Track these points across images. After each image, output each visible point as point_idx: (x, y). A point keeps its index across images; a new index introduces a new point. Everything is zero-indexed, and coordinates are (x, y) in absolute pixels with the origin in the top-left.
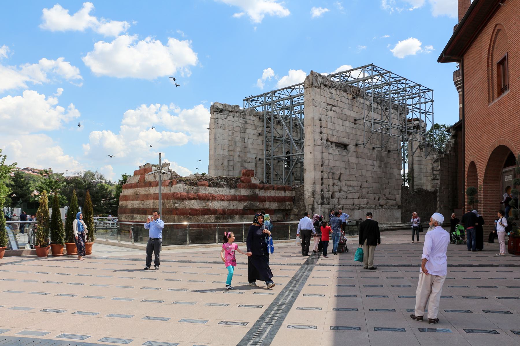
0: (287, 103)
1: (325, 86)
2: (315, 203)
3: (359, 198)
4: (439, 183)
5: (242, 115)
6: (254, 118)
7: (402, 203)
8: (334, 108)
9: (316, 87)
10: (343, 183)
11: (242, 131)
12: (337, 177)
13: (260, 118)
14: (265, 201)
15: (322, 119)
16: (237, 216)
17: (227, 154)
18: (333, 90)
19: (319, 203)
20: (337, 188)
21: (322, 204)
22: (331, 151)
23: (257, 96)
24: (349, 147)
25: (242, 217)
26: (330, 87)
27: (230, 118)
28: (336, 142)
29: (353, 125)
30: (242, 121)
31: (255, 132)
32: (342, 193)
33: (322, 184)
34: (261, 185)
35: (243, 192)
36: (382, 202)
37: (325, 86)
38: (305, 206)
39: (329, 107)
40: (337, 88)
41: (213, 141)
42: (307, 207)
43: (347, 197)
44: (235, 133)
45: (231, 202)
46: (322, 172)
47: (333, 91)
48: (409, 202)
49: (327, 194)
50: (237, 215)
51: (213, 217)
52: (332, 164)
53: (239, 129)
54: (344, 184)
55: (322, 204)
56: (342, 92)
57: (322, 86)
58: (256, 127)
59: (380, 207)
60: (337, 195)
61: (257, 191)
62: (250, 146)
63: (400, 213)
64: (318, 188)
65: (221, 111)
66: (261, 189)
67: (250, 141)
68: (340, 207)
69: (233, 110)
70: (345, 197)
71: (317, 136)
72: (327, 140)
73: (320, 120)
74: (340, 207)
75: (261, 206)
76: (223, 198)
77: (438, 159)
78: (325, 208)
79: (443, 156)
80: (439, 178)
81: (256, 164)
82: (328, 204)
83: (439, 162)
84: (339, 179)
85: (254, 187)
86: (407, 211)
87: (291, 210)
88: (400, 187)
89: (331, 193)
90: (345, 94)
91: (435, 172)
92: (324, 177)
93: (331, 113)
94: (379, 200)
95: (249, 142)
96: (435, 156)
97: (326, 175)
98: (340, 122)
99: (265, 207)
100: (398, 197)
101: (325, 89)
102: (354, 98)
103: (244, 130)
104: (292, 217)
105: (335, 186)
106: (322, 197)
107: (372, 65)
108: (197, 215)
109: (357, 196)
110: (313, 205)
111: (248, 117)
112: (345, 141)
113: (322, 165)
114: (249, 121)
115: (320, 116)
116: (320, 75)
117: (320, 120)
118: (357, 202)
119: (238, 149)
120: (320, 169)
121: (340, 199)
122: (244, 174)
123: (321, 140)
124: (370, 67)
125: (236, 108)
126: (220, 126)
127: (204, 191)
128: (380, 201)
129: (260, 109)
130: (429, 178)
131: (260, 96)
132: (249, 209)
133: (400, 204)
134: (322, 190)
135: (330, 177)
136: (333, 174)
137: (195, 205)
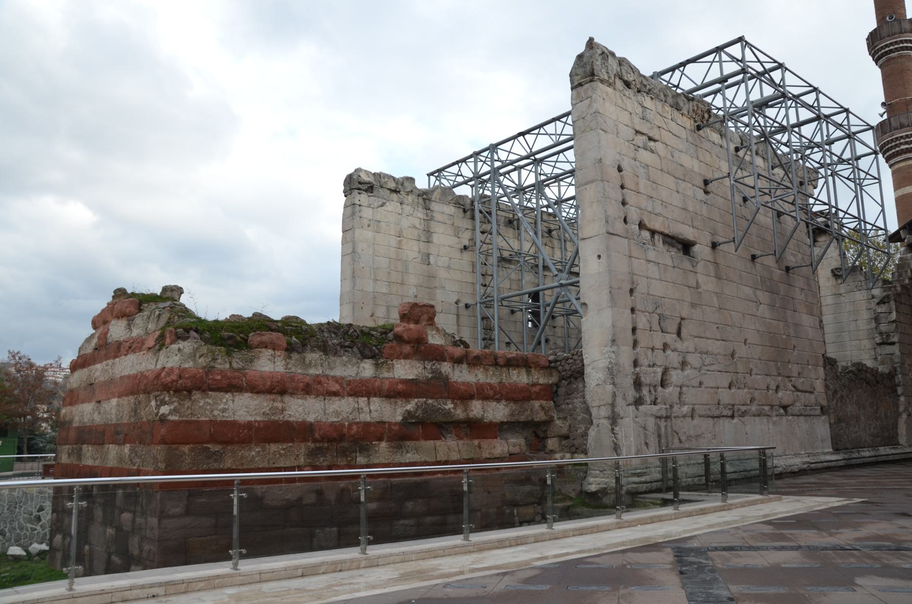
0: (528, 178)
1: (627, 84)
2: (619, 400)
3: (730, 388)
4: (898, 353)
5: (421, 200)
6: (451, 209)
7: (828, 401)
8: (652, 144)
9: (602, 81)
10: (688, 344)
11: (423, 238)
12: (674, 328)
13: (465, 211)
14: (471, 397)
15: (625, 165)
16: (383, 444)
17: (384, 290)
18: (648, 99)
19: (631, 399)
20: (674, 358)
21: (638, 402)
22: (652, 255)
23: (457, 163)
24: (696, 249)
25: (400, 447)
26: (639, 91)
27: (393, 206)
28: (662, 233)
29: (700, 194)
30: (420, 213)
31: (452, 241)
32: (688, 372)
33: (635, 344)
34: (459, 351)
35: (405, 370)
36: (785, 396)
37: (627, 84)
38: (588, 411)
39: (640, 140)
40: (657, 97)
41: (348, 258)
42: (594, 412)
43: (701, 383)
44: (405, 241)
45: (363, 401)
46: (633, 310)
47: (648, 102)
48: (842, 396)
49: (651, 376)
50: (380, 439)
51: (301, 450)
52: (658, 289)
53: (416, 232)
54: (691, 349)
55: (638, 402)
56: (668, 108)
57: (619, 84)
58: (457, 233)
59: (782, 411)
60: (675, 376)
61: (446, 368)
62: (442, 274)
63: (827, 426)
64: (626, 356)
65: (370, 188)
66: (458, 361)
67: (443, 261)
68: (685, 409)
69: (401, 187)
70: (695, 383)
71: (615, 210)
72: (642, 226)
73: (620, 169)
74: (685, 409)
75: (460, 414)
76: (335, 387)
77: (888, 296)
78: (646, 415)
79: (899, 289)
81: (458, 315)
82: (655, 403)
83: (892, 303)
84: (679, 334)
85: (437, 355)
86: (839, 420)
87: (549, 422)
88: (821, 363)
89: (659, 371)
90: (677, 114)
91: (883, 327)
92: (640, 326)
93: (644, 155)
94: (777, 391)
95: (440, 264)
96: (877, 292)
97: (644, 320)
98: (670, 181)
99: (471, 415)
100: (819, 385)
101: (627, 93)
102: (699, 128)
103: (427, 236)
104: (552, 443)
105: (669, 352)
106: (638, 384)
107: (741, 39)
108: (245, 442)
109: (725, 380)
110: (613, 405)
111: (434, 206)
112: (688, 233)
113: (632, 291)
114: (438, 216)
115: (618, 157)
116: (613, 54)
117: (620, 169)
118: (726, 396)
119: (412, 280)
120: (628, 301)
121: (684, 389)
122: (404, 317)
123: (625, 221)
124: (735, 51)
125: (406, 184)
126: (366, 222)
127: (269, 364)
128: (780, 394)
129: (465, 191)
130: (867, 344)
131: (464, 160)
132: (421, 423)
133: (824, 403)
134: (636, 364)
135: (656, 326)
136: (661, 317)
137: (243, 408)
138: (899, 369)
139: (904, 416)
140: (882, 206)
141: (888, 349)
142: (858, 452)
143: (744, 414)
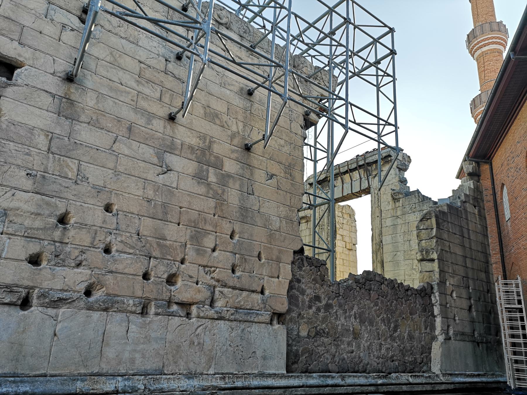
4: (437, 270)
48: (328, 307)
80: (435, 256)
133: (282, 307)
138: (436, 287)
139: (441, 338)
140: (395, 103)
141: (428, 266)
142: (343, 378)
143: (57, 303)
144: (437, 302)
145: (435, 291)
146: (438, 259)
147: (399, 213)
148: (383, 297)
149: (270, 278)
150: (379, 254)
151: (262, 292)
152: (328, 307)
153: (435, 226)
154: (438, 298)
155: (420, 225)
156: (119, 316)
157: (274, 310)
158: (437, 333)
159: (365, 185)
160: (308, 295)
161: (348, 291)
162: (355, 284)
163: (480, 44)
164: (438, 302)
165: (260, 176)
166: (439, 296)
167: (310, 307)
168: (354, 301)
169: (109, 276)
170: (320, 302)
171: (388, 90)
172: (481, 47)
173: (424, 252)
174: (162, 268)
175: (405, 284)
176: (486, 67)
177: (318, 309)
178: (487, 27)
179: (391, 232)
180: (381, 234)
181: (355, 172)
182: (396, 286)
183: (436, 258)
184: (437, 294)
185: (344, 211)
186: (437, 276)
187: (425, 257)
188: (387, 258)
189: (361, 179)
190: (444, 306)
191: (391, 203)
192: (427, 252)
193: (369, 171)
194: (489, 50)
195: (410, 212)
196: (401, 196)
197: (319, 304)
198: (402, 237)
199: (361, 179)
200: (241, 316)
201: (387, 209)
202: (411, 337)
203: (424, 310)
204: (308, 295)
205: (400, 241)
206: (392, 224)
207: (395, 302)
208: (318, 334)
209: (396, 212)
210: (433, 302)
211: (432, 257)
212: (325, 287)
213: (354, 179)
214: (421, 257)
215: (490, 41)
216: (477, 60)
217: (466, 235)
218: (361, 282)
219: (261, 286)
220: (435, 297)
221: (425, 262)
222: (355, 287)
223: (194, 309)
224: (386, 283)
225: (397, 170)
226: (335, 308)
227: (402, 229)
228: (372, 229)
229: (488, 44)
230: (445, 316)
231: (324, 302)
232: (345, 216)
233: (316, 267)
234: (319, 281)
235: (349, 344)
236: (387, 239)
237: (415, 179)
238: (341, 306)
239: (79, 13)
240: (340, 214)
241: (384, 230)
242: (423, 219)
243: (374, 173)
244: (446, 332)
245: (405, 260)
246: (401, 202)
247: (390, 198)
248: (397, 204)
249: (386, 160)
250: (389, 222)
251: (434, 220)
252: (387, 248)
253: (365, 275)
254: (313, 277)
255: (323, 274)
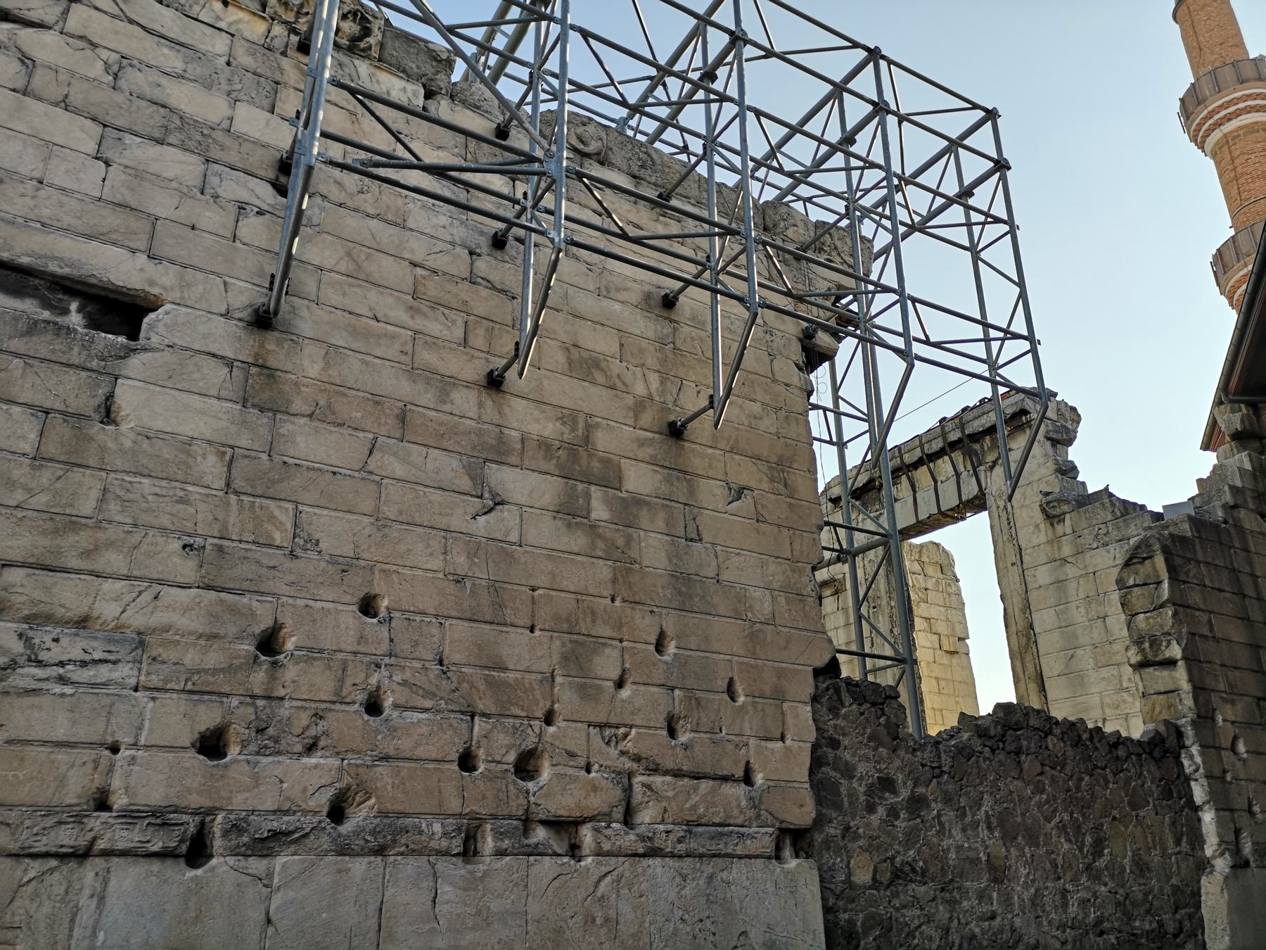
4: (1185, 686)
48: (916, 804)
80: (1176, 651)
133: (802, 812)
138: (1189, 732)
139: (1222, 865)
140: (1021, 283)
141: (1160, 678)
143: (268, 844)
144: (1197, 770)
145: (1188, 743)
146: (1184, 658)
147: (1067, 550)
148: (1053, 768)
149: (763, 743)
150: (1028, 657)
151: (747, 779)
152: (916, 804)
153: (1164, 575)
154: (1198, 760)
155: (1125, 575)
156: (412, 866)
157: (782, 822)
158: (1209, 852)
159: (970, 489)
160: (861, 778)
161: (963, 760)
162: (979, 742)
163: (1216, 117)
164: (1201, 770)
165: (712, 494)
166: (1202, 754)
167: (871, 808)
168: (981, 784)
169: (382, 769)
170: (895, 792)
171: (1000, 255)
172: (1219, 124)
173: (1147, 645)
174: (502, 739)
175: (1109, 729)
176: (1239, 170)
177: (893, 813)
178: (1228, 73)
179: (1052, 601)
180: (1027, 607)
181: (940, 461)
182: (1085, 736)
183: (1179, 656)
184: (1195, 750)
185: (925, 558)
186: (1189, 702)
187: (1150, 657)
188: (1051, 667)
189: (958, 475)
190: (1216, 779)
191: (1042, 526)
192: (1155, 643)
193: (977, 454)
194: (1241, 128)
195: (1095, 546)
196: (1066, 508)
197: (891, 799)
198: (1082, 610)
199: (958, 475)
200: (703, 842)
201: (1035, 541)
202: (1141, 867)
203: (1167, 794)
204: (861, 778)
205: (1080, 620)
206: (1052, 580)
207: (1087, 778)
208: (897, 875)
209: (1059, 549)
210: (1187, 771)
211: (1168, 654)
212: (902, 753)
213: (940, 479)
214: (1139, 658)
215: (1241, 105)
216: (1213, 156)
217: (1250, 591)
218: (992, 733)
219: (743, 764)
220: (1191, 757)
221: (1151, 670)
222: (980, 749)
223: (587, 835)
224: (1057, 731)
225: (1048, 443)
226: (933, 805)
227: (1081, 590)
228: (1002, 598)
229: (1237, 114)
230: (1224, 807)
231: (904, 794)
232: (930, 570)
233: (874, 704)
234: (887, 739)
235: (982, 896)
236: (1044, 619)
237: (1098, 463)
238: (951, 800)
239: (271, 175)
240: (917, 567)
241: (1033, 596)
242: (1130, 559)
243: (990, 458)
244: (1231, 845)
245: (1099, 666)
246: (1068, 522)
247: (1039, 517)
248: (1059, 529)
249: (1016, 423)
250: (1043, 576)
251: (1160, 561)
252: (1048, 642)
253: (1001, 715)
254: (869, 731)
255: (894, 720)
